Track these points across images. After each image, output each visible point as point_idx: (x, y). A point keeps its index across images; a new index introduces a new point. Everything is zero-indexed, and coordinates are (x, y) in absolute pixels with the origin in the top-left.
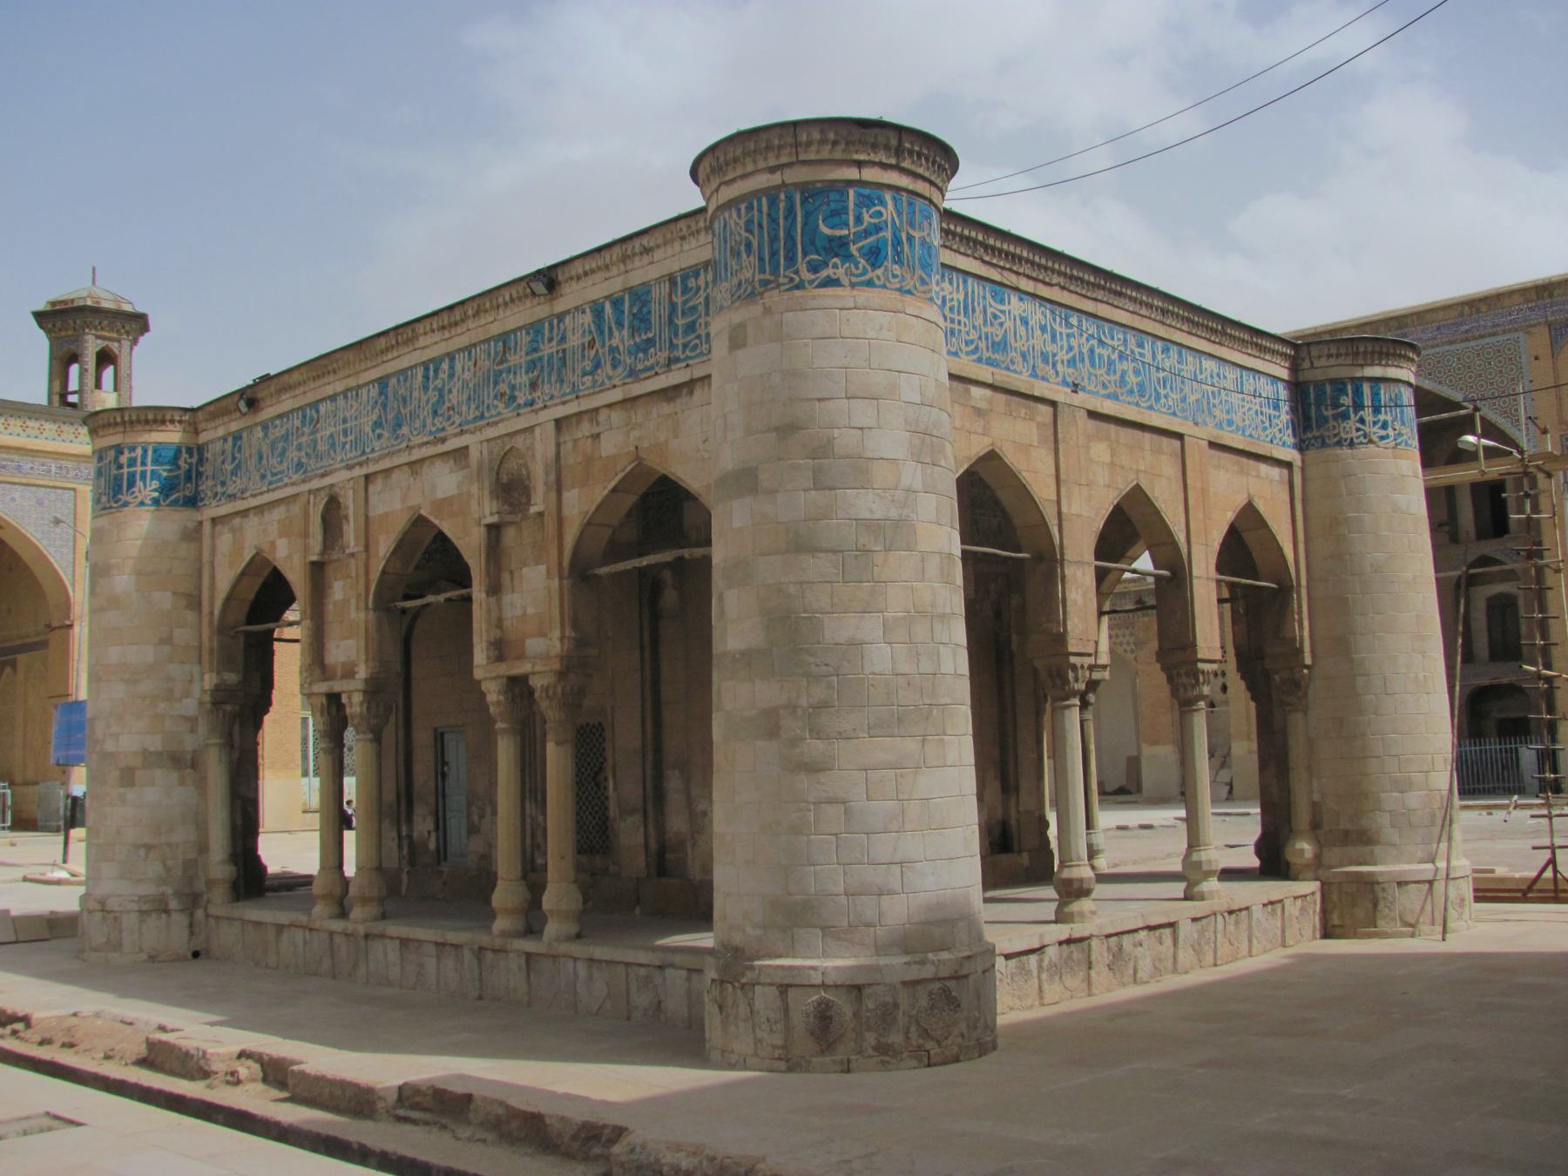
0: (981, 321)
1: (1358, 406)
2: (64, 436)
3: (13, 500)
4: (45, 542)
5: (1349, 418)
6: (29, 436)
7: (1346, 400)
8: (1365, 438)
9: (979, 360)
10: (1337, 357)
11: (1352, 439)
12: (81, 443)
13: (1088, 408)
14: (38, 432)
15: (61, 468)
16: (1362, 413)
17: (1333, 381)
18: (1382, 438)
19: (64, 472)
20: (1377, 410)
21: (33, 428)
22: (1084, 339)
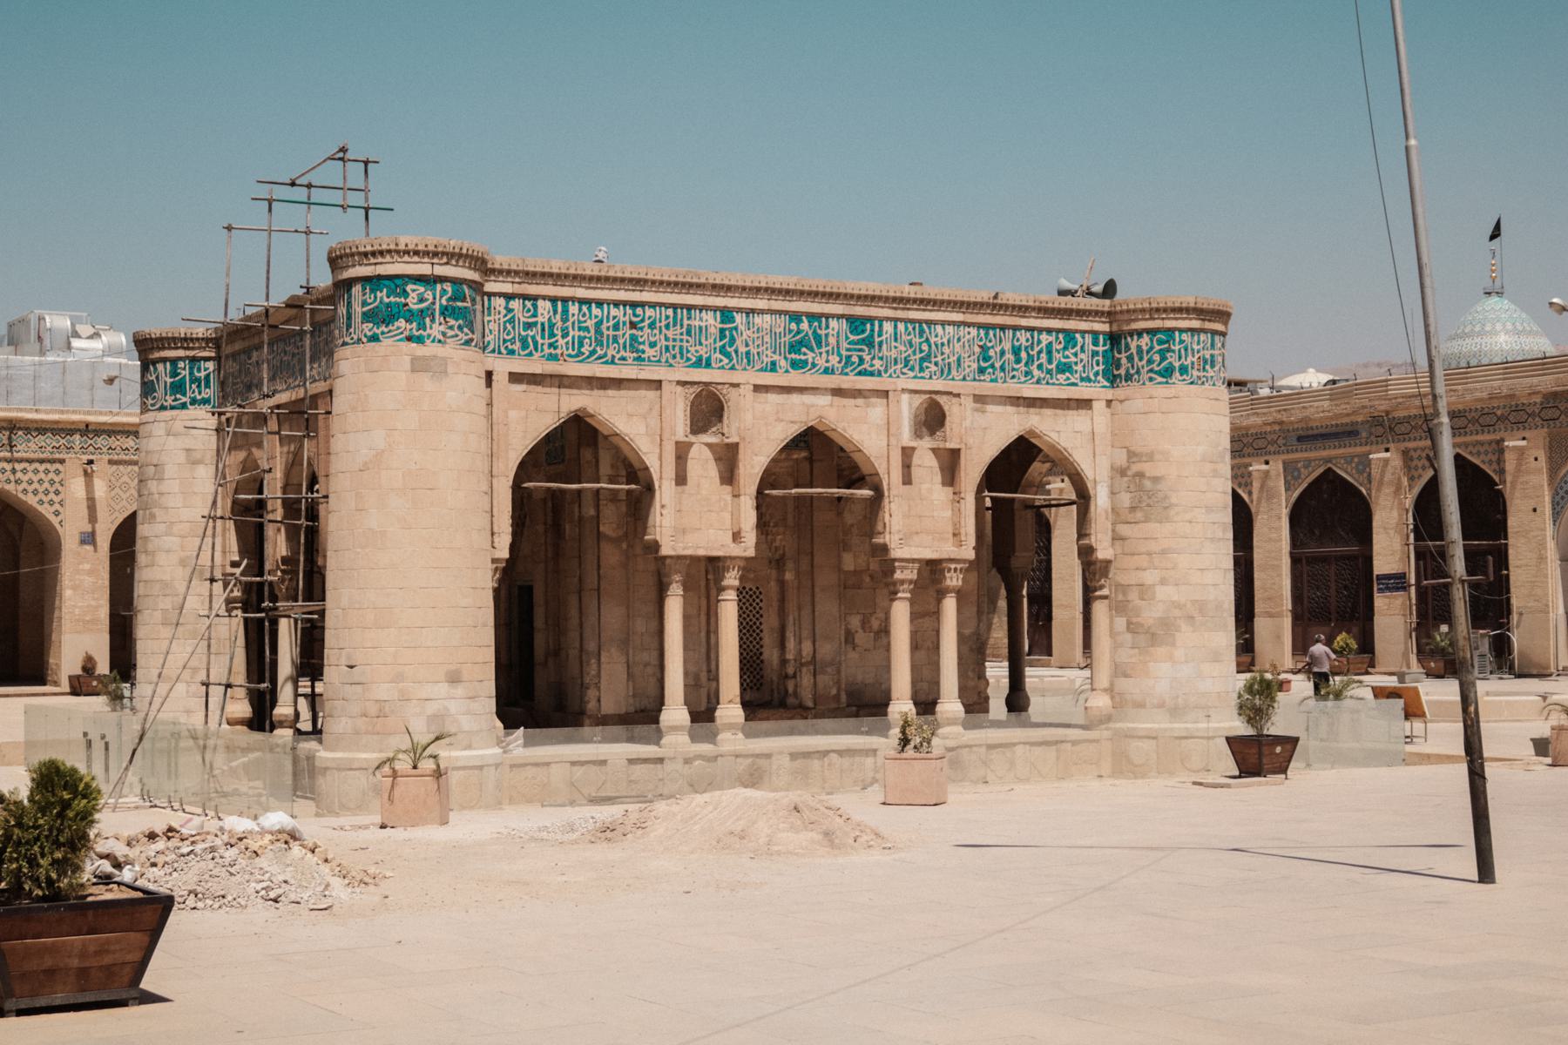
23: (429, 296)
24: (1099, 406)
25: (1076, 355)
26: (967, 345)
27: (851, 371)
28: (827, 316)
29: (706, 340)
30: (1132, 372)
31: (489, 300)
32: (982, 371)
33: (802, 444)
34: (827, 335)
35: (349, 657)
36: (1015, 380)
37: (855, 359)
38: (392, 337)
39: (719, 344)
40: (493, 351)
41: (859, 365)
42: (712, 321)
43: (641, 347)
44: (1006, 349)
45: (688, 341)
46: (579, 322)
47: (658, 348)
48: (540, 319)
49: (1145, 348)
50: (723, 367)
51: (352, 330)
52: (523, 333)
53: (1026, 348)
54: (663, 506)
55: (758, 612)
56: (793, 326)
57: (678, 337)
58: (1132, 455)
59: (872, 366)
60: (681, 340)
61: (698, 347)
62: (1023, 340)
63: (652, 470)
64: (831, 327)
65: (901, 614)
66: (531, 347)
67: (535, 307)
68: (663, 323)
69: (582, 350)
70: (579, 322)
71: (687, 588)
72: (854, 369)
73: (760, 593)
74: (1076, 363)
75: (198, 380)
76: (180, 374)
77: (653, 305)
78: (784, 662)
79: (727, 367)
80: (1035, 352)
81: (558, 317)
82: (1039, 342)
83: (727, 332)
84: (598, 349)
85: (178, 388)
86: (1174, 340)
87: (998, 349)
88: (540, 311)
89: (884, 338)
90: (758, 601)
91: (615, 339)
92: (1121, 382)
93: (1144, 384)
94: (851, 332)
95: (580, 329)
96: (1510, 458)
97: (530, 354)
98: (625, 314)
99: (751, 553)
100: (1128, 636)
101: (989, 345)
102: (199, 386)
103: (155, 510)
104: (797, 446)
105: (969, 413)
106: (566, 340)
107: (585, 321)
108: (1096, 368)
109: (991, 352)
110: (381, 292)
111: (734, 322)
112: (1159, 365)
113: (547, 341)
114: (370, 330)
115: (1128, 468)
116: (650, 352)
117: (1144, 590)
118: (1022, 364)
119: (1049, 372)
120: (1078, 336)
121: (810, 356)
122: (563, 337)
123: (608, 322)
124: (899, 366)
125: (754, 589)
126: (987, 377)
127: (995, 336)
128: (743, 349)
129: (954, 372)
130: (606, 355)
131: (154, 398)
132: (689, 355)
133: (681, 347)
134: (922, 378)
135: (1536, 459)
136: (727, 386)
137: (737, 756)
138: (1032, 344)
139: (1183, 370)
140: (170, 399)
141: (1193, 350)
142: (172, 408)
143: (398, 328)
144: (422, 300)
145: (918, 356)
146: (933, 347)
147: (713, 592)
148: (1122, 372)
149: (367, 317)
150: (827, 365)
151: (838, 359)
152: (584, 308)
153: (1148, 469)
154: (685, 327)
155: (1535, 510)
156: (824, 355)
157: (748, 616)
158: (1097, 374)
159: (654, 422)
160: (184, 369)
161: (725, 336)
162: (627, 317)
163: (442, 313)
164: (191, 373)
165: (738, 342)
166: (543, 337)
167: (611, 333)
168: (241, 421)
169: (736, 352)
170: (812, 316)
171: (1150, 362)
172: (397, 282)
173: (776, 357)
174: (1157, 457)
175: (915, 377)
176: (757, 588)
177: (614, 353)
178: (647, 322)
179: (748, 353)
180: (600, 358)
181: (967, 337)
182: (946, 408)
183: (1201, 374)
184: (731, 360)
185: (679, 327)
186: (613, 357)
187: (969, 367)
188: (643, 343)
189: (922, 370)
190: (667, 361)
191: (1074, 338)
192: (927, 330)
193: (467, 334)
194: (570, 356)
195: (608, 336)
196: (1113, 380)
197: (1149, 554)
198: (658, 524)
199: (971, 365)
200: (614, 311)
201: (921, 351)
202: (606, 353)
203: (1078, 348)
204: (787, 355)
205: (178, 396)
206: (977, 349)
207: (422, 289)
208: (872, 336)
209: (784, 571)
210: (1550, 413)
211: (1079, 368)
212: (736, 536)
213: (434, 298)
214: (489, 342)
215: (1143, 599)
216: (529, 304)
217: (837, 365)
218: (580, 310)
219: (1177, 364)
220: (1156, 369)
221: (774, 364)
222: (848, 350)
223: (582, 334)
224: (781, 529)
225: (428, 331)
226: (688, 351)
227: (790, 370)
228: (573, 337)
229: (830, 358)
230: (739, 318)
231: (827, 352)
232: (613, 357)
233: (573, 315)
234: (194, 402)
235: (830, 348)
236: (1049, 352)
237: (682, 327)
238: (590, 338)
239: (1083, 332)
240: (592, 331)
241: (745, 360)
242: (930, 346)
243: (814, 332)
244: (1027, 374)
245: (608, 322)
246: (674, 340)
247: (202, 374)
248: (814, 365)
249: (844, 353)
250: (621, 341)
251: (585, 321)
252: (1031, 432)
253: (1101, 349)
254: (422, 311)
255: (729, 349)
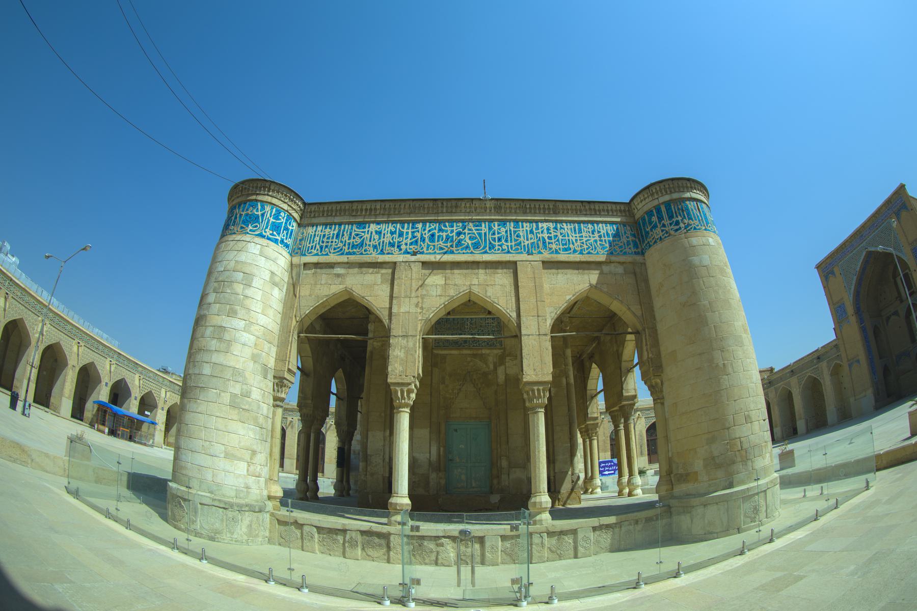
0: (347, 238)
1: (660, 218)
5: (657, 227)
7: (655, 219)
8: (667, 234)
9: (342, 254)
10: (645, 200)
11: (660, 237)
13: (422, 261)
16: (663, 221)
17: (646, 213)
18: (677, 230)
20: (671, 217)
22: (426, 231)
76: (280, 219)
102: (287, 234)
103: (238, 308)
131: (256, 227)
140: (268, 232)
160: (283, 218)
164: (286, 223)
168: (333, 268)
205: (275, 233)
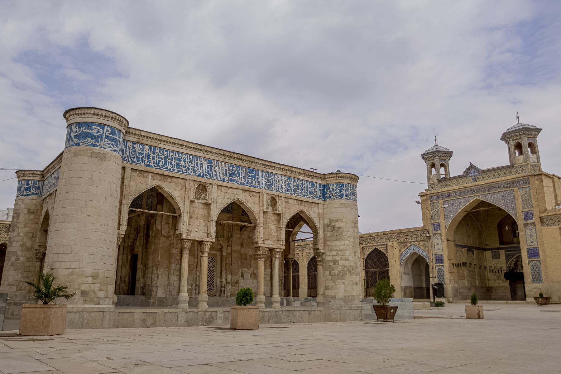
2: (507, 174)
3: (494, 198)
4: (506, 208)
6: (496, 178)
12: (513, 175)
14: (493, 177)
15: (507, 184)
19: (509, 185)
21: (514, 172)
23: (101, 131)
24: (321, 206)
25: (314, 189)
26: (284, 183)
27: (249, 185)
28: (242, 167)
29: (203, 168)
30: (331, 195)
31: (127, 143)
32: (288, 190)
33: (230, 212)
34: (242, 173)
35: (52, 265)
36: (297, 195)
37: (250, 181)
38: (84, 144)
39: (207, 170)
40: (126, 160)
41: (251, 183)
42: (205, 162)
43: (180, 167)
44: (295, 185)
45: (196, 168)
46: (159, 155)
47: (186, 168)
48: (145, 152)
49: (335, 189)
50: (207, 178)
51: (70, 142)
52: (138, 156)
53: (301, 185)
54: (184, 222)
55: (213, 265)
56: (231, 168)
57: (193, 166)
58: (331, 221)
59: (255, 184)
60: (194, 167)
61: (200, 170)
62: (300, 183)
63: (181, 209)
64: (243, 170)
65: (262, 264)
66: (141, 161)
67: (143, 148)
68: (188, 161)
69: (159, 165)
70: (159, 155)
71: (190, 255)
72: (250, 184)
73: (214, 259)
74: (314, 192)
75: (35, 188)
77: (185, 154)
78: (221, 282)
79: (209, 178)
80: (303, 187)
81: (152, 152)
82: (304, 184)
83: (210, 167)
84: (165, 165)
85: (28, 189)
86: (344, 186)
87: (293, 185)
88: (145, 149)
89: (259, 176)
90: (213, 262)
91: (171, 163)
92: (327, 199)
93: (334, 199)
94: (249, 173)
95: (159, 158)
96: (389, 247)
97: (140, 163)
98: (175, 156)
99: (214, 240)
100: (330, 277)
101: (290, 183)
102: (35, 189)
104: (228, 212)
105: (284, 203)
106: (154, 161)
107: (161, 156)
108: (320, 194)
109: (291, 185)
110: (83, 128)
111: (212, 164)
112: (339, 194)
113: (147, 160)
114: (76, 141)
115: (330, 224)
116: (183, 169)
117: (335, 262)
118: (299, 190)
119: (307, 193)
120: (315, 184)
121: (236, 178)
122: (153, 159)
123: (169, 157)
124: (264, 186)
125: (212, 258)
126: (289, 192)
127: (292, 181)
128: (214, 173)
129: (280, 190)
130: (167, 168)
132: (196, 172)
133: (194, 169)
134: (270, 190)
135: (396, 249)
136: (208, 184)
137: (205, 312)
138: (302, 184)
139: (346, 195)
140: (25, 192)
141: (349, 190)
142: (25, 195)
143: (88, 141)
144: (98, 132)
145: (269, 183)
146: (274, 181)
147: (200, 254)
148: (328, 195)
149: (76, 137)
150: (241, 182)
151: (245, 181)
152: (161, 151)
153: (337, 225)
154: (196, 163)
155: (396, 261)
156: (240, 179)
157: (210, 266)
158: (320, 196)
159: (183, 193)
161: (209, 168)
162: (176, 156)
163: (106, 138)
165: (213, 171)
166: (145, 158)
167: (170, 161)
169: (212, 173)
170: (238, 166)
171: (336, 192)
172: (88, 125)
173: (225, 177)
174: (339, 220)
175: (268, 190)
176: (213, 258)
177: (171, 168)
178: (183, 160)
179: (216, 174)
180: (165, 168)
181: (284, 180)
182: (277, 200)
183: (352, 197)
184: (210, 176)
185: (193, 163)
186: (170, 169)
187: (284, 189)
188: (181, 166)
189: (270, 188)
190: (189, 173)
191: (314, 185)
192: (272, 176)
193: (115, 148)
194: (155, 166)
195: (169, 161)
196: (324, 198)
197: (337, 250)
198: (182, 227)
199: (285, 188)
200: (171, 154)
201: (270, 182)
202: (168, 167)
203: (315, 187)
204: (229, 177)
205: (28, 192)
206: (286, 184)
207: (99, 128)
208: (256, 175)
209: (222, 252)
210: (399, 238)
211: (315, 193)
212: (208, 235)
213: (103, 132)
214: (125, 157)
215: (335, 265)
216: (141, 147)
217: (244, 182)
218: (160, 152)
219: (344, 194)
220: (338, 195)
221: (224, 179)
222: (248, 178)
223: (160, 159)
224: (222, 239)
225: (99, 143)
226: (196, 171)
227: (229, 182)
228: (156, 160)
229: (243, 180)
230: (213, 163)
231: (242, 178)
232: (170, 169)
233: (157, 153)
234: (33, 194)
235: (242, 177)
236: (307, 188)
237: (195, 163)
238: (162, 161)
239: (317, 183)
240: (163, 159)
241: (215, 177)
242: (273, 181)
243: (238, 171)
244: (301, 193)
245: (169, 157)
246: (192, 167)
247: (37, 185)
248: (237, 181)
249: (246, 179)
250: (173, 164)
251: (161, 156)
252: (301, 211)
253: (321, 189)
254: (98, 135)
255: (210, 172)
